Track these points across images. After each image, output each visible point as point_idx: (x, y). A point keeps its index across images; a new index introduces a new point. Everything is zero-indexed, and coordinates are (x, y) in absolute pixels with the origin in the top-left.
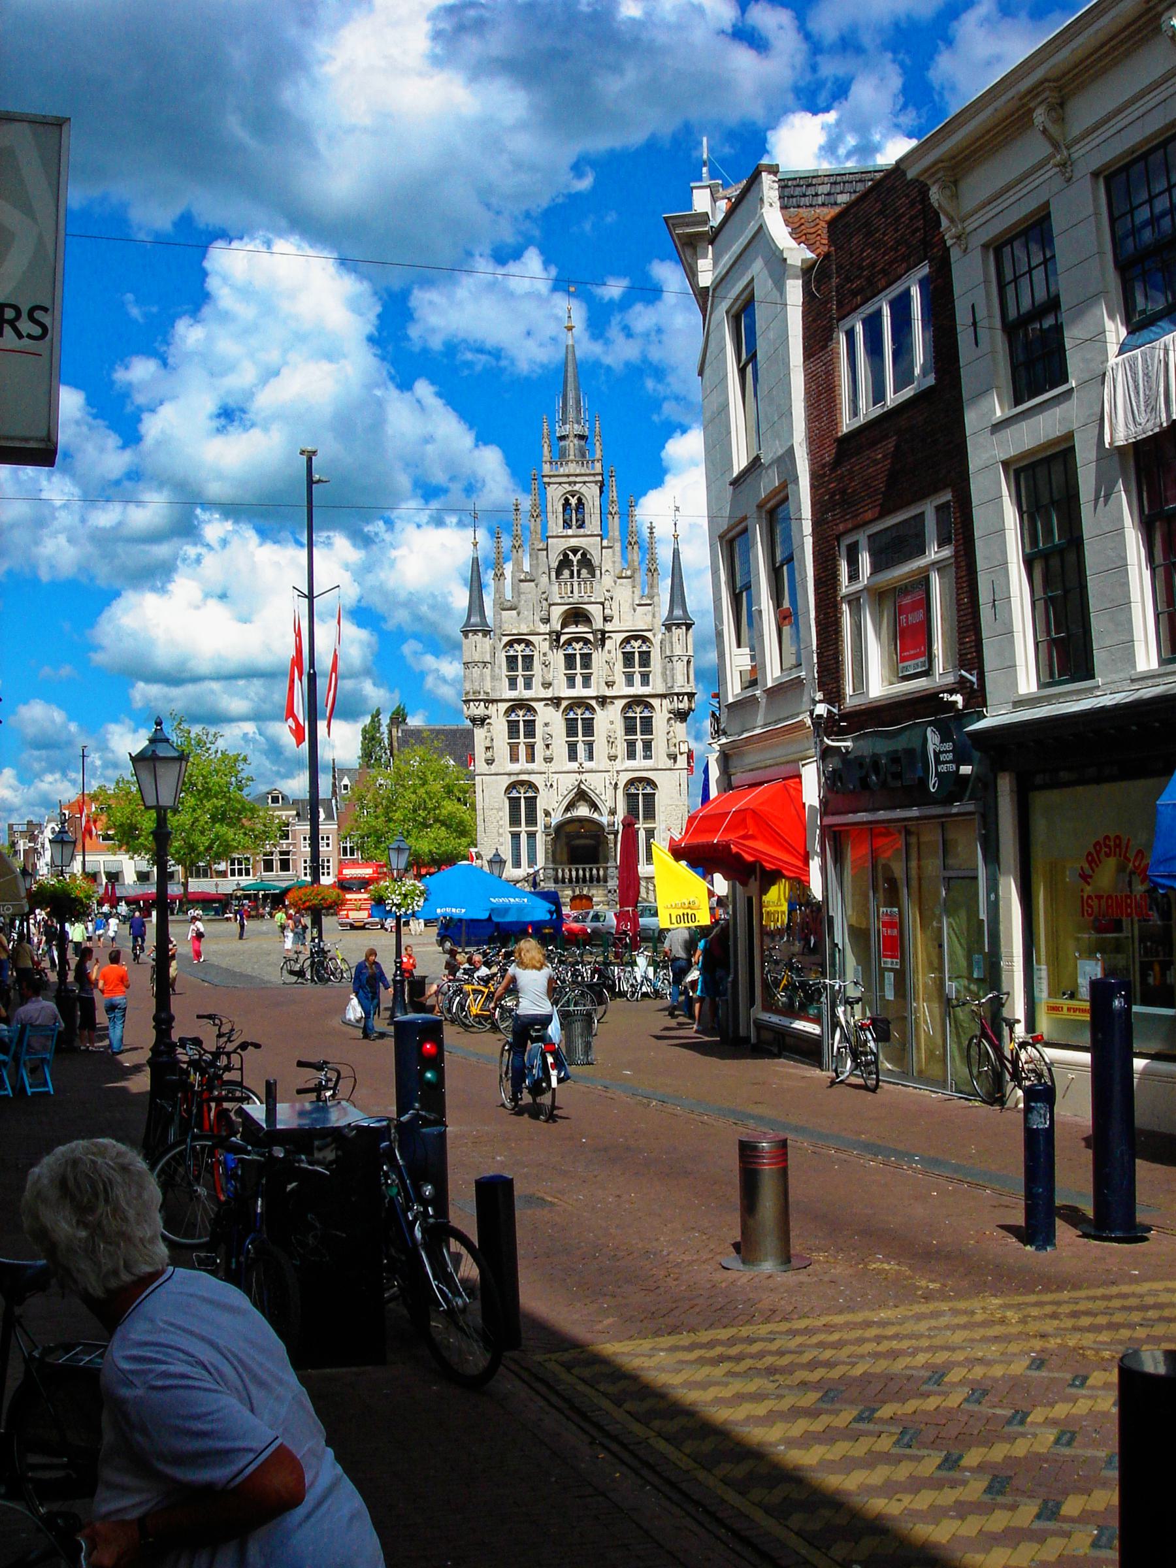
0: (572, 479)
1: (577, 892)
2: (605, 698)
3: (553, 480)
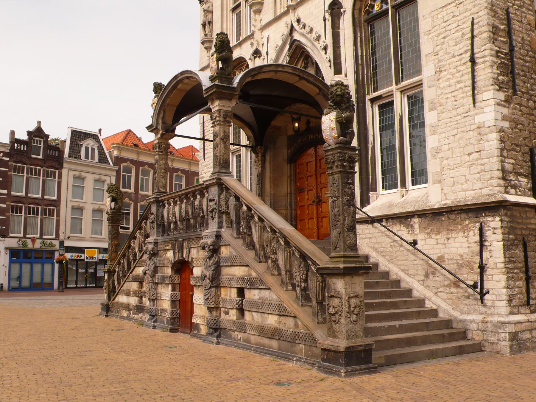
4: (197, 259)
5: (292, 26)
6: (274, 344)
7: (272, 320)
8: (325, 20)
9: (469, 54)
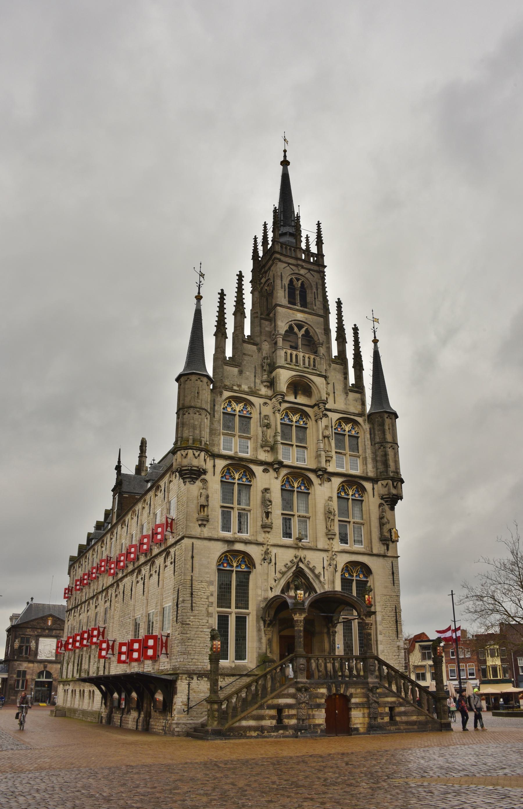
0: (300, 263)
1: (334, 691)
2: (325, 471)
3: (283, 258)
4: (356, 694)
5: (300, 558)
6: (415, 727)
7: (414, 718)
8: (324, 568)
9: (395, 618)
